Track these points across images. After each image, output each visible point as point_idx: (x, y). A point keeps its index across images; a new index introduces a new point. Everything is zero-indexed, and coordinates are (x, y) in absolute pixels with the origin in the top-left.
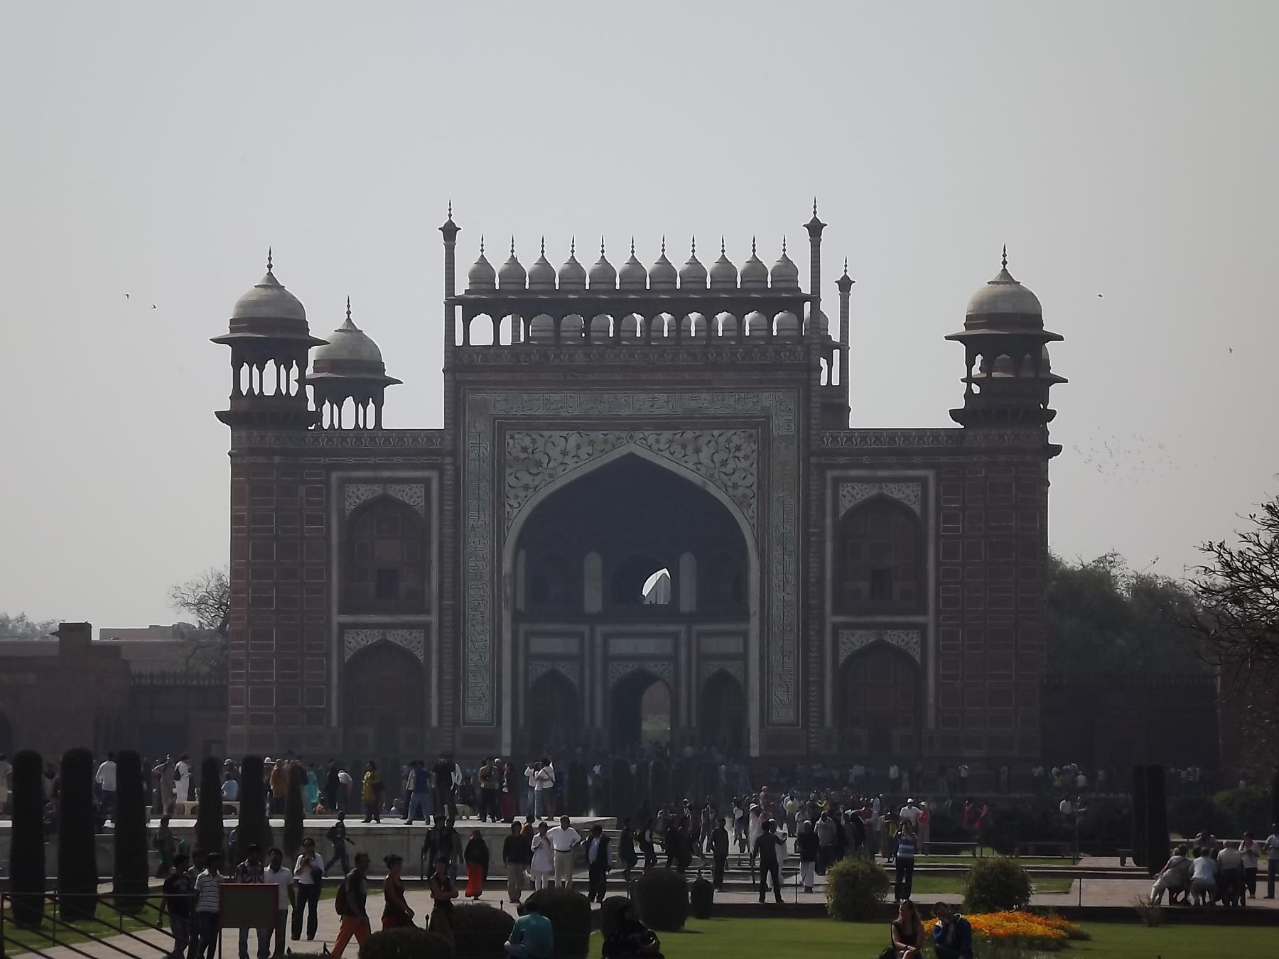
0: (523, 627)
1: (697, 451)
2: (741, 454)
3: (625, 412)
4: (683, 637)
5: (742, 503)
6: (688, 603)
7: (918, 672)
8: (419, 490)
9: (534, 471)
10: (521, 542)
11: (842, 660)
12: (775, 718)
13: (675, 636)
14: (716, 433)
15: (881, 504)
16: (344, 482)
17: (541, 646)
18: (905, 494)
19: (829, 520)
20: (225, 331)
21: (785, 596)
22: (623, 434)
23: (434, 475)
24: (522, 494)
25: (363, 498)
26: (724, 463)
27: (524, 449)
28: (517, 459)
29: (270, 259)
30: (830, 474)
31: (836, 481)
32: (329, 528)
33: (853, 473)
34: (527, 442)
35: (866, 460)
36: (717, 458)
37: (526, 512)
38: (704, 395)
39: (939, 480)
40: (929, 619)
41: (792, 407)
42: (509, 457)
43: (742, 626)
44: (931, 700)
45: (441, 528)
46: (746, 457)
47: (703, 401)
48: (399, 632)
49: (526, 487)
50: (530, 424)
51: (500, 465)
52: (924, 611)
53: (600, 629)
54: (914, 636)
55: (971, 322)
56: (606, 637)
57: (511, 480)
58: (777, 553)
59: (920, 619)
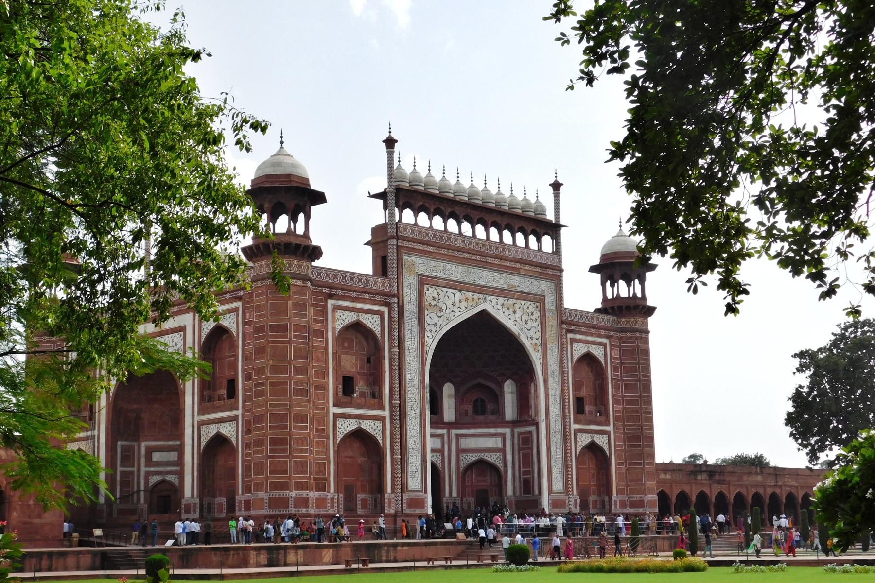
1: (515, 312)
3: (481, 282)
4: (446, 437)
9: (439, 314)
12: (555, 489)
13: (441, 436)
14: (523, 302)
16: (336, 308)
21: (555, 410)
22: (481, 296)
24: (434, 329)
25: (346, 321)
26: (526, 322)
27: (434, 299)
28: (430, 304)
29: (282, 137)
30: (570, 336)
33: (578, 337)
34: (435, 294)
35: (583, 329)
36: (524, 320)
38: (517, 278)
39: (611, 346)
40: (610, 428)
42: (426, 303)
43: (500, 430)
45: (390, 349)
46: (536, 320)
48: (368, 422)
50: (435, 282)
51: (421, 308)
52: (608, 424)
54: (606, 437)
57: (427, 318)
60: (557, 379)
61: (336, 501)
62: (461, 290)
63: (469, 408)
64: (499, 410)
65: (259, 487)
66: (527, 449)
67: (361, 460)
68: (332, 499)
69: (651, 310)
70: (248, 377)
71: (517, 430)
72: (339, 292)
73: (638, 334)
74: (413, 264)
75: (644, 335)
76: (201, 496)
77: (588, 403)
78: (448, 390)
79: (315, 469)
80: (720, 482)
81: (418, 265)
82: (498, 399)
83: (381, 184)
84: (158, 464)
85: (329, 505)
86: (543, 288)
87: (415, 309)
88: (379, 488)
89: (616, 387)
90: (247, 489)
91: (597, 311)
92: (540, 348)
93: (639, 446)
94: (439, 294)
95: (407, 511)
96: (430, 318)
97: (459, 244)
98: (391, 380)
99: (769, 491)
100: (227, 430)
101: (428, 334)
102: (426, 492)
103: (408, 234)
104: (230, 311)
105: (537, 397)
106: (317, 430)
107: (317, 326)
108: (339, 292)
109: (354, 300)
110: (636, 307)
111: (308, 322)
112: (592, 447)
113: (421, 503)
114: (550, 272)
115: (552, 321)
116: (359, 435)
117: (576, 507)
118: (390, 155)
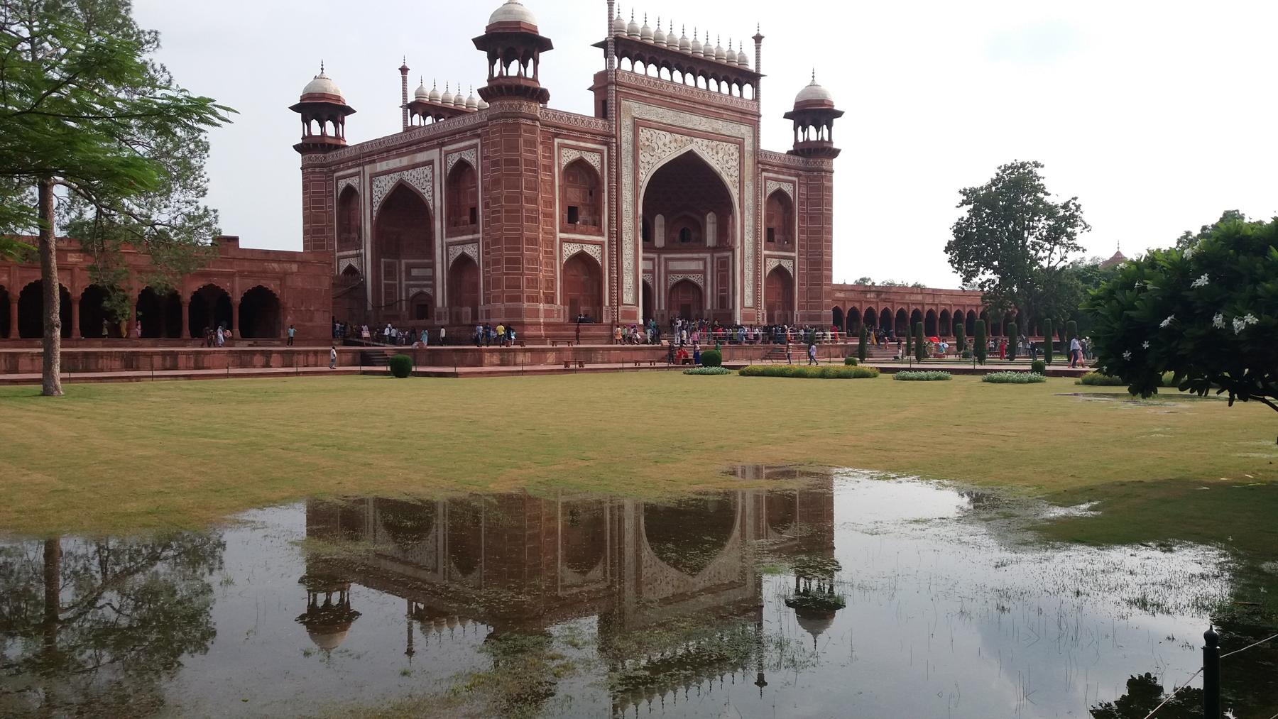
3: (690, 126)
7: (791, 281)
13: (653, 259)
16: (562, 146)
18: (787, 188)
21: (749, 238)
43: (702, 255)
50: (649, 125)
62: (671, 132)
63: (677, 236)
64: (701, 238)
65: (497, 299)
66: (724, 272)
67: (583, 278)
69: (835, 153)
70: (486, 206)
71: (716, 255)
72: (565, 132)
76: (450, 305)
77: (778, 231)
78: (659, 220)
79: (543, 285)
80: (885, 301)
81: (633, 109)
82: (701, 229)
83: (603, 35)
84: (416, 278)
87: (630, 148)
88: (600, 302)
89: (802, 220)
90: (487, 301)
91: (789, 153)
95: (621, 321)
96: (644, 157)
97: (671, 90)
98: (610, 208)
99: (927, 308)
100: (470, 251)
103: (626, 80)
104: (470, 147)
105: (734, 226)
107: (546, 162)
108: (565, 132)
109: (577, 139)
110: (824, 149)
112: (780, 271)
113: (634, 316)
115: (749, 162)
116: (581, 258)
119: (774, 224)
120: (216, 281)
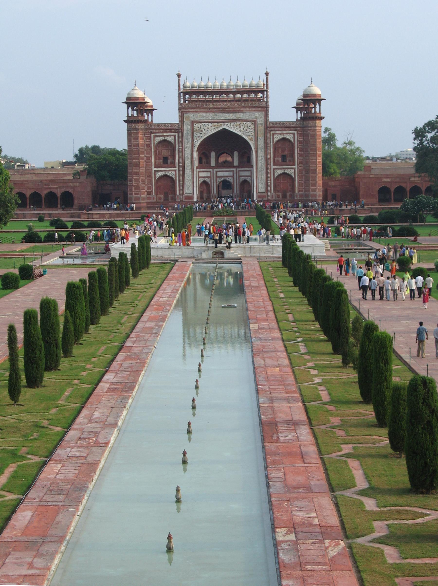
0: (198, 170)
1: (240, 127)
2: (250, 128)
3: (222, 119)
4: (235, 171)
5: (251, 139)
6: (236, 163)
7: (293, 180)
8: (173, 138)
10: (198, 150)
11: (275, 177)
12: (260, 191)
13: (233, 171)
14: (244, 123)
15: (284, 139)
17: (202, 174)
19: (272, 143)
20: (125, 100)
21: (261, 162)
23: (177, 134)
24: (198, 138)
26: (246, 130)
27: (198, 128)
28: (196, 130)
30: (272, 132)
31: (273, 134)
32: (151, 147)
33: (277, 132)
34: (199, 126)
35: (280, 129)
36: (245, 129)
37: (199, 142)
39: (298, 134)
40: (296, 167)
41: (263, 116)
43: (250, 169)
44: (297, 186)
45: (179, 146)
46: (252, 129)
47: (242, 115)
49: (199, 137)
50: (199, 122)
52: (294, 164)
53: (215, 170)
54: (293, 171)
55: (304, 96)
56: (217, 172)
57: (195, 135)
58: (259, 151)
59: (294, 167)
60: (262, 150)
61: (155, 198)
62: (211, 122)
68: (154, 198)
72: (156, 131)
73: (309, 128)
74: (189, 117)
75: (313, 128)
85: (152, 199)
86: (256, 116)
87: (189, 132)
92: (254, 139)
93: (308, 173)
94: (200, 126)
95: (184, 200)
101: (195, 140)
102: (194, 194)
106: (147, 176)
107: (147, 143)
108: (156, 131)
111: (139, 144)
114: (260, 109)
115: (261, 129)
117: (272, 197)
118: (179, 79)
119: (286, 153)
120: (52, 190)
